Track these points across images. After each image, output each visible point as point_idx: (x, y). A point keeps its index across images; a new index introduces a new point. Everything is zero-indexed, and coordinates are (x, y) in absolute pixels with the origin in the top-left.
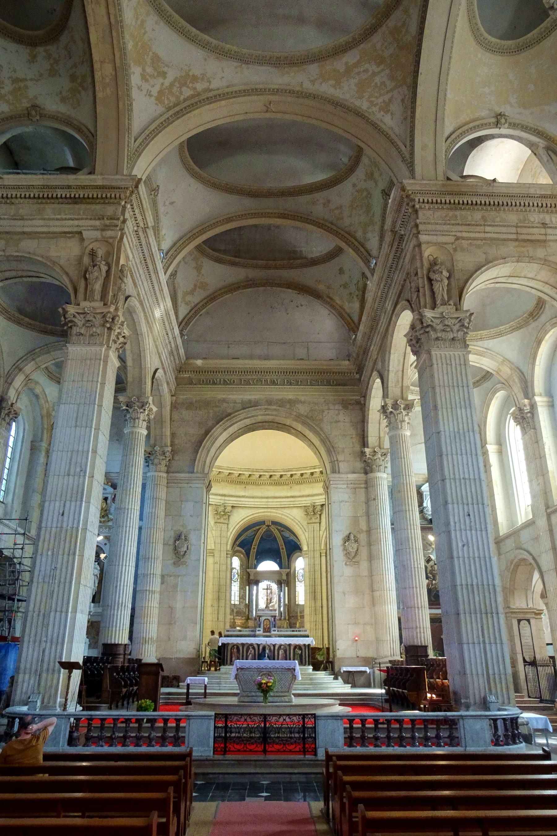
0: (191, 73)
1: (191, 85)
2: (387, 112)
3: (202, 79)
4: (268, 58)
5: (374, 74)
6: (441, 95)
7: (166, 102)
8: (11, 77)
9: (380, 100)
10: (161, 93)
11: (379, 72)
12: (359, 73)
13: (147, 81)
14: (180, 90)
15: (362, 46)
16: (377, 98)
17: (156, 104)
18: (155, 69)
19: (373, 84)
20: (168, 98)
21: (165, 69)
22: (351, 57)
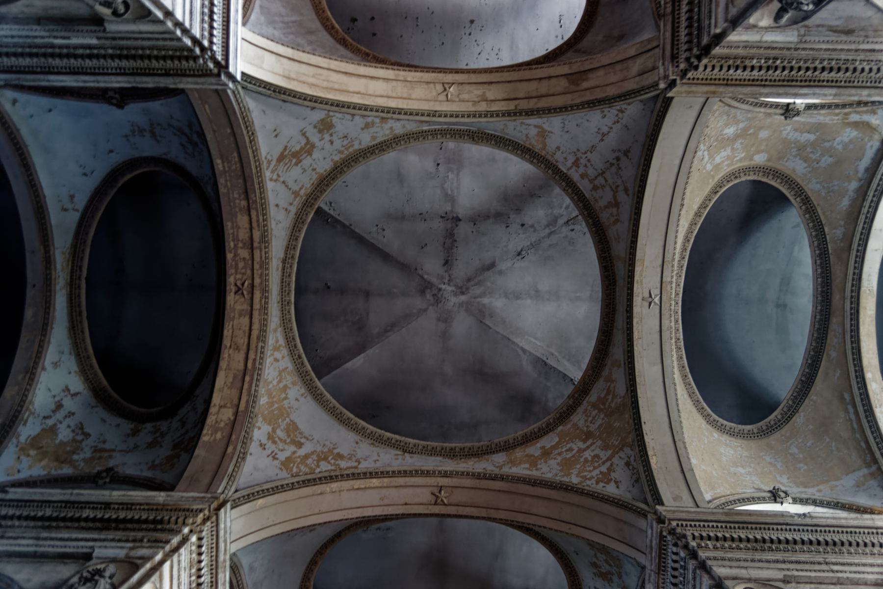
0: (336, 451)
1: (333, 461)
2: (608, 483)
3: (350, 459)
4: (438, 449)
5: (581, 451)
6: (679, 444)
7: (295, 470)
8: (96, 447)
9: (597, 472)
10: (289, 460)
11: (588, 448)
12: (559, 454)
13: (275, 442)
14: (318, 464)
15: (560, 428)
16: (590, 471)
17: (281, 469)
18: (289, 436)
19: (582, 460)
20: (297, 467)
21: (303, 440)
22: (548, 441)
